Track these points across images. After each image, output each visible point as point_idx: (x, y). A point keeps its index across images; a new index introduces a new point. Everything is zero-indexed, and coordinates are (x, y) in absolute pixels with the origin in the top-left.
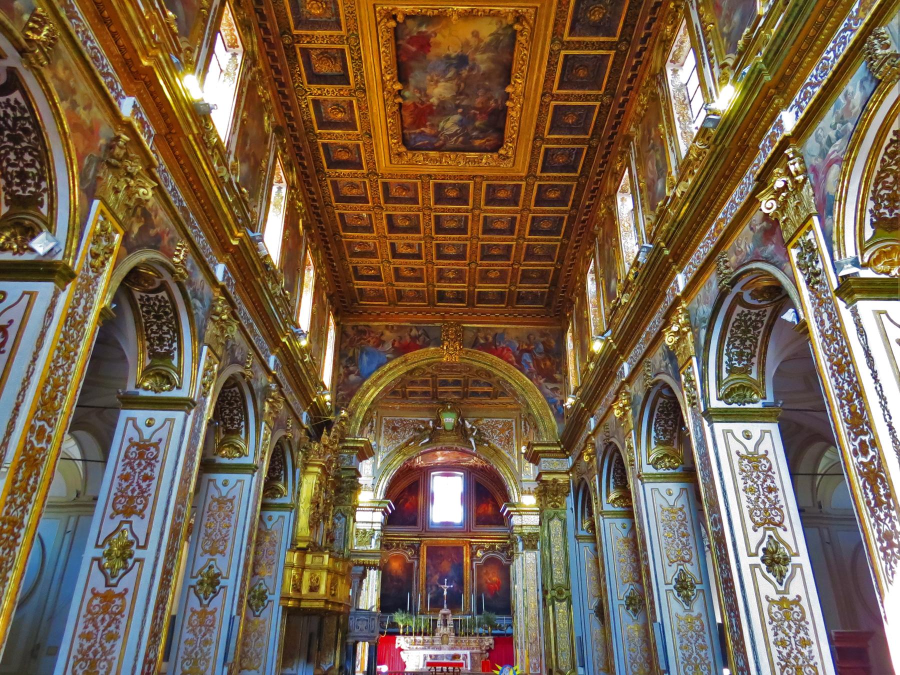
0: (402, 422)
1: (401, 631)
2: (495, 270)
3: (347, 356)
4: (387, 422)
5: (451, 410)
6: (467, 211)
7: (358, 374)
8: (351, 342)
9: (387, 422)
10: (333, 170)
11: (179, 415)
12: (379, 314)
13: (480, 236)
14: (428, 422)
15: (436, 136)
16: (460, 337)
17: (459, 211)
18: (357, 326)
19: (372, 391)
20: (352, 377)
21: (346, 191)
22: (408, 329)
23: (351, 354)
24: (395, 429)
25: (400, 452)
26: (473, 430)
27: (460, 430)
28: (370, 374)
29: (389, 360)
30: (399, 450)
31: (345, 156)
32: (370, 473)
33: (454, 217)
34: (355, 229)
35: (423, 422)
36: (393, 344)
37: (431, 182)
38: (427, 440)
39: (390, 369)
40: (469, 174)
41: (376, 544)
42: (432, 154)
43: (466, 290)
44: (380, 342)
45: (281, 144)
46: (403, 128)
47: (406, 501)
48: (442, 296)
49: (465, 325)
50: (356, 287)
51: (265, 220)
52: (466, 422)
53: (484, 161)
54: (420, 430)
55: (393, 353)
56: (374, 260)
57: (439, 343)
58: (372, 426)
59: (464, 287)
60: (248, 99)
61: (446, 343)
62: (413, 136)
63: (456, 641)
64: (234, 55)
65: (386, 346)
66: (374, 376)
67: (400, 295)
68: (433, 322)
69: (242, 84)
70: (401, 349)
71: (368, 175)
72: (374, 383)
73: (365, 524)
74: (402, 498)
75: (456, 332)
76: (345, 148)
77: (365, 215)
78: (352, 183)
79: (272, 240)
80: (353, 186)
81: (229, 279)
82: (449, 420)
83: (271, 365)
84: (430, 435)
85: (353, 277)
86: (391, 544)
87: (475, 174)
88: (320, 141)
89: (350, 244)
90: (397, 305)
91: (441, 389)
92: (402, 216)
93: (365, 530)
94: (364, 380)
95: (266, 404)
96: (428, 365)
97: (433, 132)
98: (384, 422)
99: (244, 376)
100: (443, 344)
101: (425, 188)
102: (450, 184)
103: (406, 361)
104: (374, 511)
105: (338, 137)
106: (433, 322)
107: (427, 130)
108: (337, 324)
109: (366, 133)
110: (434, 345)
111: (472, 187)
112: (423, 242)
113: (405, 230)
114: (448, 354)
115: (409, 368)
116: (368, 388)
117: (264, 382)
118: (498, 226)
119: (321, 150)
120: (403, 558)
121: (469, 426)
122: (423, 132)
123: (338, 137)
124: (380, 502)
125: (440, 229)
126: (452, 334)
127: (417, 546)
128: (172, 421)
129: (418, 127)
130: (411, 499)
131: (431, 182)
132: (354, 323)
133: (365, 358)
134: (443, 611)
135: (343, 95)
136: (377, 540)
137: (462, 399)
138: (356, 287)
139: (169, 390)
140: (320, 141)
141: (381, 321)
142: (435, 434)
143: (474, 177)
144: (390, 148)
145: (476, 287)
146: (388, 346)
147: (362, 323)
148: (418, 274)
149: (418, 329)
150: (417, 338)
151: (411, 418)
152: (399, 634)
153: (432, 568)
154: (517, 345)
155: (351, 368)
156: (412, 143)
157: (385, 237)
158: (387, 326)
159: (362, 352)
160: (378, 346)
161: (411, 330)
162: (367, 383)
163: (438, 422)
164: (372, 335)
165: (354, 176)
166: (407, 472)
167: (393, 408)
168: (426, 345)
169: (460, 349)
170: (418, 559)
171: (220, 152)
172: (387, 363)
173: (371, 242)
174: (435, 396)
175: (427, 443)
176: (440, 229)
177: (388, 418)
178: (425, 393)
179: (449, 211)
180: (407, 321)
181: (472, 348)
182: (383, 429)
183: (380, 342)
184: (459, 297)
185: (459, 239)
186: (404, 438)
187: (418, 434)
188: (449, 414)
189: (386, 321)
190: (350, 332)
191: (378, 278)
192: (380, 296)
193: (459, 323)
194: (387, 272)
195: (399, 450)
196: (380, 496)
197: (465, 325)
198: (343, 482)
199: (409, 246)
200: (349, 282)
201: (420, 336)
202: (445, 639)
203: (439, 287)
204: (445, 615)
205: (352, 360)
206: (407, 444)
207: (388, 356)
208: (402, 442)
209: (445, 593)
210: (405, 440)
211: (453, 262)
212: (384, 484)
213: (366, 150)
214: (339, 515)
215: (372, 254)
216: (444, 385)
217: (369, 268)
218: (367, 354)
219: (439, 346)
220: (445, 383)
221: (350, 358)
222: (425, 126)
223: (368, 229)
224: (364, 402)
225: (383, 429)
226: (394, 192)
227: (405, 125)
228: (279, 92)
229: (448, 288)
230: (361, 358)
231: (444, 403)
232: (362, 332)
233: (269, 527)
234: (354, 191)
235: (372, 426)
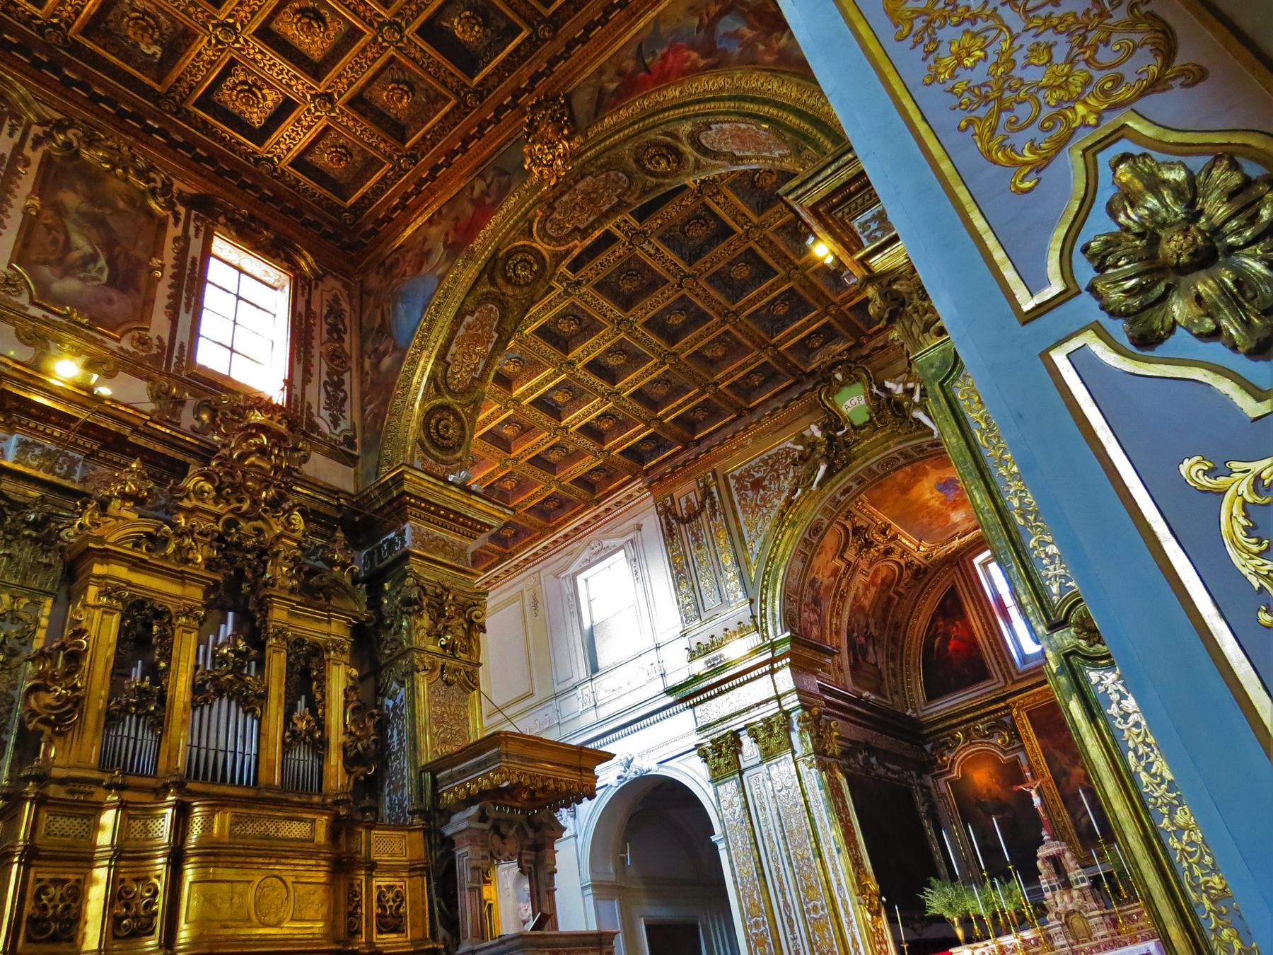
0: (765, 462)
1: (960, 933)
4: (739, 479)
5: (850, 380)
9: (739, 479)
20: (387, 362)
24: (757, 485)
26: (910, 392)
27: (890, 411)
38: (823, 468)
41: (803, 741)
47: (946, 638)
52: (888, 384)
54: (803, 458)
58: (713, 505)
63: (1115, 923)
73: (764, 708)
74: (935, 636)
82: (853, 403)
93: (766, 720)
98: (732, 482)
104: (772, 672)
121: (898, 389)
127: (1007, 720)
130: (956, 631)
133: (401, 308)
134: (1042, 852)
136: (801, 733)
137: (858, 345)
152: (956, 943)
153: (1058, 754)
154: (696, 21)
155: (382, 348)
163: (833, 421)
170: (1022, 748)
175: (829, 474)
177: (737, 473)
178: (768, 374)
186: (780, 491)
188: (845, 391)
202: (1076, 922)
204: (1055, 861)
206: (789, 503)
208: (779, 503)
209: (1037, 801)
210: (783, 496)
225: (736, 498)
235: (713, 505)
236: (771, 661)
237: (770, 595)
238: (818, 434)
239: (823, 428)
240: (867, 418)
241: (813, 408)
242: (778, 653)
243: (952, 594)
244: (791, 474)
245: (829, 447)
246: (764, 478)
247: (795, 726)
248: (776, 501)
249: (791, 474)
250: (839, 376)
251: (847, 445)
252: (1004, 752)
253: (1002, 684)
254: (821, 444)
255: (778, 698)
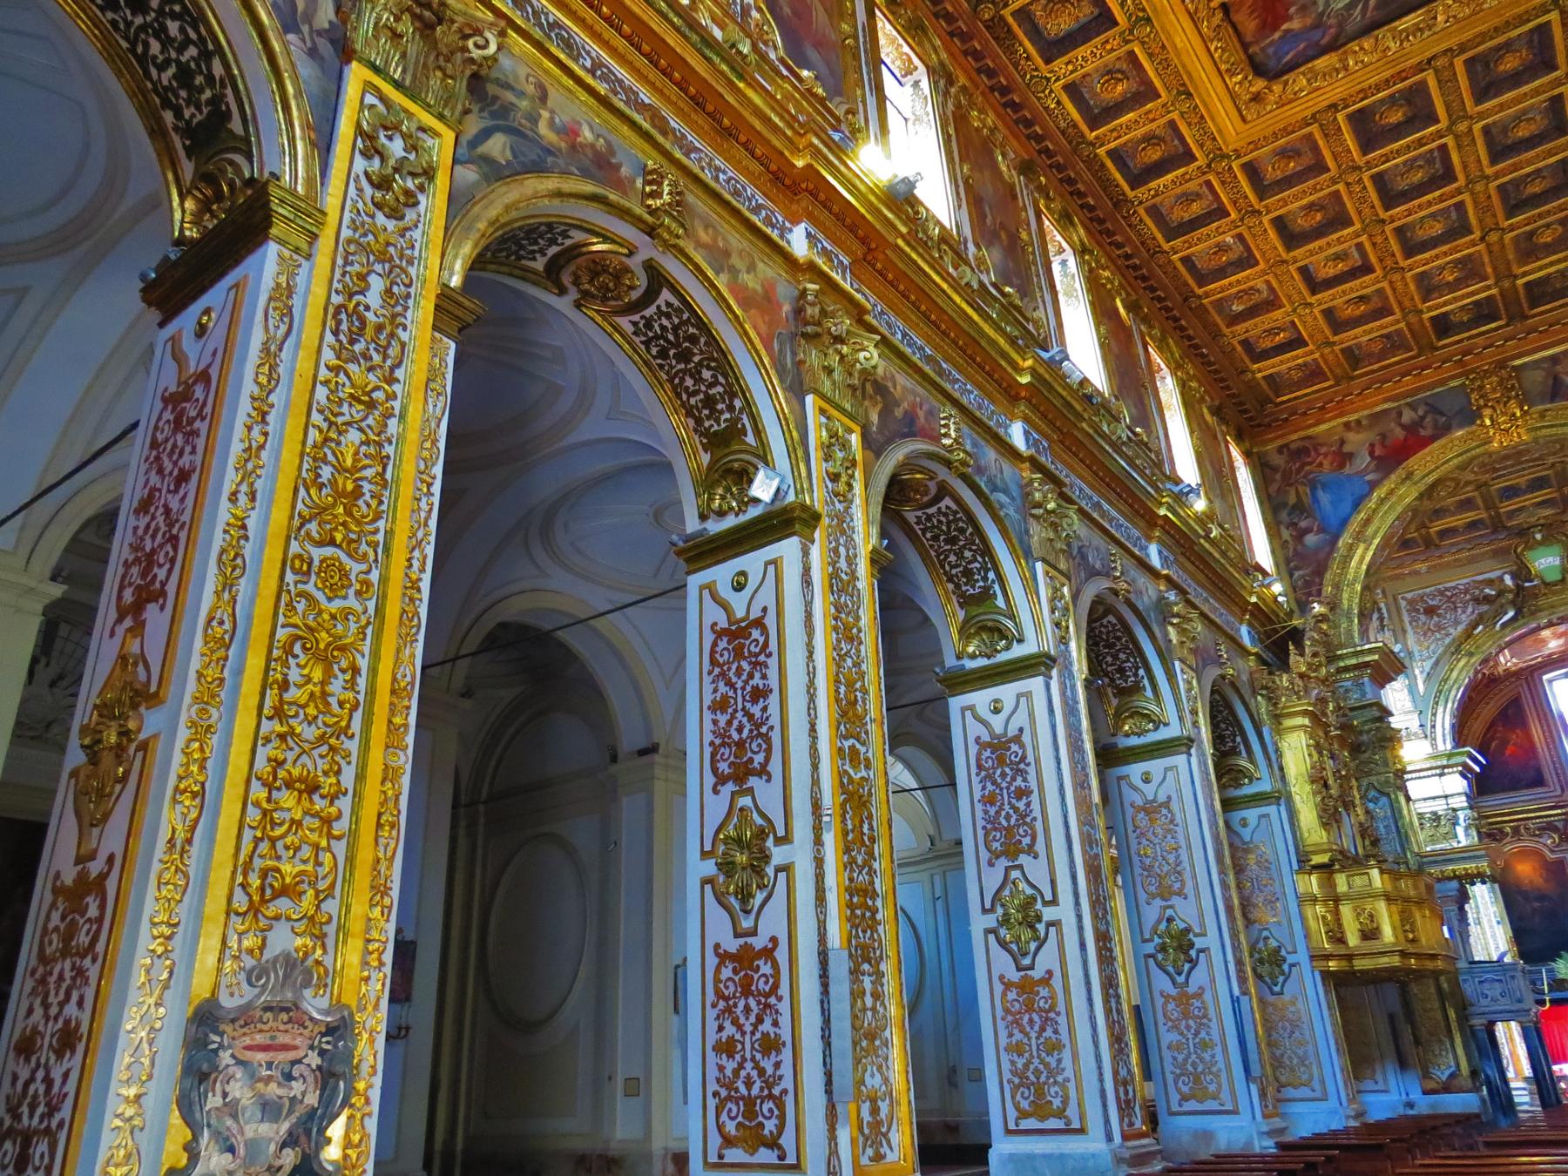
0: (1442, 593)
2: (1548, 226)
3: (1286, 504)
4: (1411, 602)
5: (1545, 542)
6: (1439, 135)
7: (1321, 530)
8: (1286, 476)
9: (1411, 602)
10: (1142, 189)
11: (1035, 684)
12: (1322, 408)
13: (1489, 171)
14: (1501, 579)
15: (1318, 25)
16: (1514, 386)
17: (1421, 143)
18: (1286, 446)
19: (1359, 552)
20: (1311, 539)
21: (1181, 214)
22: (1394, 415)
23: (1292, 499)
24: (1430, 611)
25: (1458, 650)
28: (1344, 523)
29: (1373, 485)
30: (1456, 649)
31: (1154, 154)
32: (1409, 705)
33: (1415, 159)
34: (1221, 273)
35: (1490, 583)
36: (1371, 454)
37: (1340, 117)
38: (1511, 614)
39: (1382, 501)
40: (1418, 59)
41: (1467, 835)
42: (1321, 63)
43: (1494, 291)
44: (1343, 458)
45: (1041, 189)
46: (1245, 46)
47: (1504, 743)
48: (1443, 326)
49: (1518, 362)
50: (1259, 375)
51: (1060, 325)
53: (1439, 18)
54: (1487, 599)
55: (1377, 469)
56: (1278, 314)
57: (1470, 416)
58: (1381, 619)
59: (1488, 288)
60: (964, 145)
61: (1487, 412)
62: (1271, 51)
64: (916, 84)
65: (1358, 461)
66: (1354, 525)
67: (1353, 357)
68: (1443, 382)
69: (944, 125)
70: (1392, 456)
71: (1209, 166)
72: (1359, 537)
74: (1492, 739)
75: (1501, 383)
76: (1149, 139)
77: (1229, 240)
78: (1185, 194)
79: (1083, 352)
80: (1189, 198)
81: (1036, 443)
83: (1155, 561)
84: (1513, 603)
85: (1247, 360)
86: (1501, 831)
87: (1429, 54)
88: (1101, 151)
89: (1219, 304)
90: (1353, 378)
91: (1506, 507)
92: (1303, 208)
93: (1435, 813)
94: (1336, 538)
95: (1170, 629)
96: (1462, 467)
97: (1309, 21)
98: (1403, 603)
99: (1116, 593)
100: (1481, 417)
101: (1332, 132)
102: (1382, 101)
103: (1409, 475)
104: (1441, 775)
105: (1130, 126)
106: (1443, 382)
107: (1295, 24)
108: (1247, 455)
109: (1179, 93)
110: (1461, 426)
111: (1432, 83)
112: (1364, 238)
113: (1319, 232)
114: (1504, 430)
115: (1422, 487)
116: (1351, 548)
117: (1152, 593)
118: (1523, 132)
119: (1109, 164)
120: (1538, 854)
122: (1287, 31)
123: (1130, 126)
124: (1450, 756)
125: (1390, 198)
126: (1494, 390)
128: (1028, 695)
129: (1275, 28)
131: (1340, 117)
132: (1280, 442)
133: (1324, 498)
135: (1112, 50)
136: (1467, 829)
138: (1259, 375)
139: (1007, 648)
140: (1101, 151)
141: (1330, 420)
142: (1526, 599)
143: (1429, 61)
144: (1233, 97)
145: (1516, 277)
146: (1363, 460)
147: (1295, 437)
148: (1376, 303)
149: (1412, 407)
150: (1419, 423)
151: (1460, 580)
155: (1303, 524)
156: (1272, 63)
157: (1284, 262)
158: (1347, 425)
159: (1314, 489)
160: (1342, 466)
161: (1400, 414)
162: (1345, 540)
163: (1522, 572)
164: (1323, 450)
165: (1185, 179)
166: (1487, 686)
167: (1417, 573)
168: (1442, 431)
169: (1525, 413)
171: (951, 247)
172: (1371, 492)
173: (1259, 284)
174: (1497, 525)
176: (1390, 198)
177: (1409, 596)
178: (1473, 525)
179: (1399, 153)
180: (1386, 400)
181: (1552, 400)
182: (1406, 619)
183: (1343, 458)
184: (1484, 312)
185: (1441, 199)
186: (1457, 623)
187: (1485, 608)
189: (1341, 415)
190: (1278, 460)
191: (1297, 342)
192: (1313, 374)
193: (1502, 364)
194: (1310, 321)
195: (1456, 649)
196: (1445, 744)
197: (1518, 362)
198: (1361, 733)
199: (1338, 257)
200: (1243, 372)
201: (1422, 418)
203: (1430, 309)
205: (1299, 508)
206: (1468, 634)
207: (1368, 478)
210: (1460, 628)
211: (1445, 248)
212: (1444, 719)
213: (1189, 124)
214: (1373, 793)
215: (1272, 304)
216: (1508, 498)
217: (1272, 332)
218: (1324, 487)
219: (1473, 423)
220: (1511, 492)
221: (1294, 507)
222: (1289, 18)
223: (1247, 261)
224: (1350, 577)
225: (1406, 619)
226: (1271, 174)
227: (1248, 39)
228: (1005, 105)
229: (1450, 304)
230: (1316, 500)
231: (1523, 533)
232: (1300, 453)
233: (1247, 838)
234: (1195, 206)
235: (1381, 619)
236: (1444, 767)
237: (1440, 710)
238: (1508, 580)
239: (1514, 576)
240: (1559, 577)
241: (1498, 554)
242: (1452, 761)
243: (1516, 702)
244: (1470, 609)
245: (1517, 595)
246: (1439, 607)
247: (1461, 821)
248: (1452, 630)
249: (1470, 609)
250: (1538, 537)
251: (1536, 596)
252: (1552, 851)
253: (1559, 792)
254: (1511, 591)
255: (1446, 797)
